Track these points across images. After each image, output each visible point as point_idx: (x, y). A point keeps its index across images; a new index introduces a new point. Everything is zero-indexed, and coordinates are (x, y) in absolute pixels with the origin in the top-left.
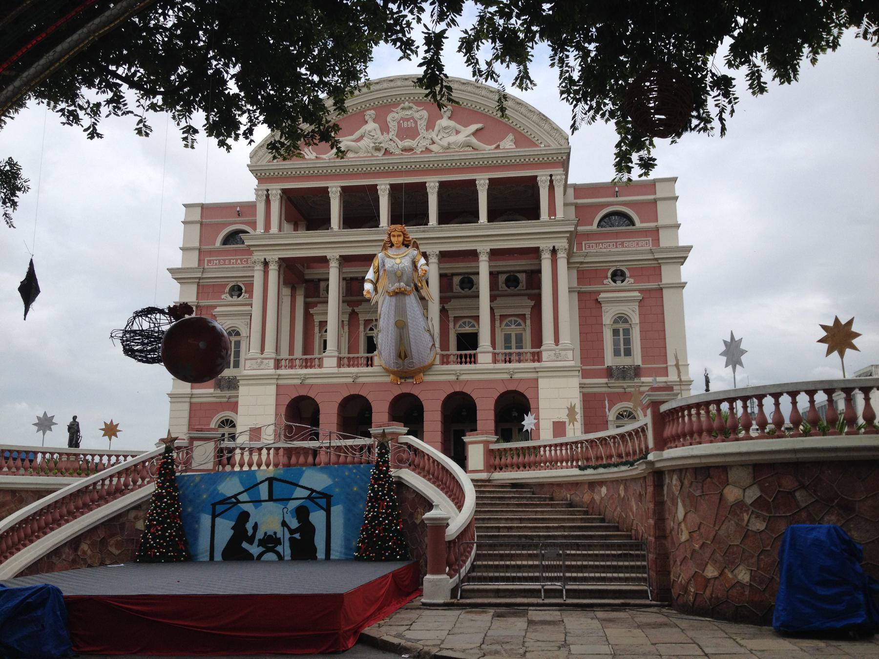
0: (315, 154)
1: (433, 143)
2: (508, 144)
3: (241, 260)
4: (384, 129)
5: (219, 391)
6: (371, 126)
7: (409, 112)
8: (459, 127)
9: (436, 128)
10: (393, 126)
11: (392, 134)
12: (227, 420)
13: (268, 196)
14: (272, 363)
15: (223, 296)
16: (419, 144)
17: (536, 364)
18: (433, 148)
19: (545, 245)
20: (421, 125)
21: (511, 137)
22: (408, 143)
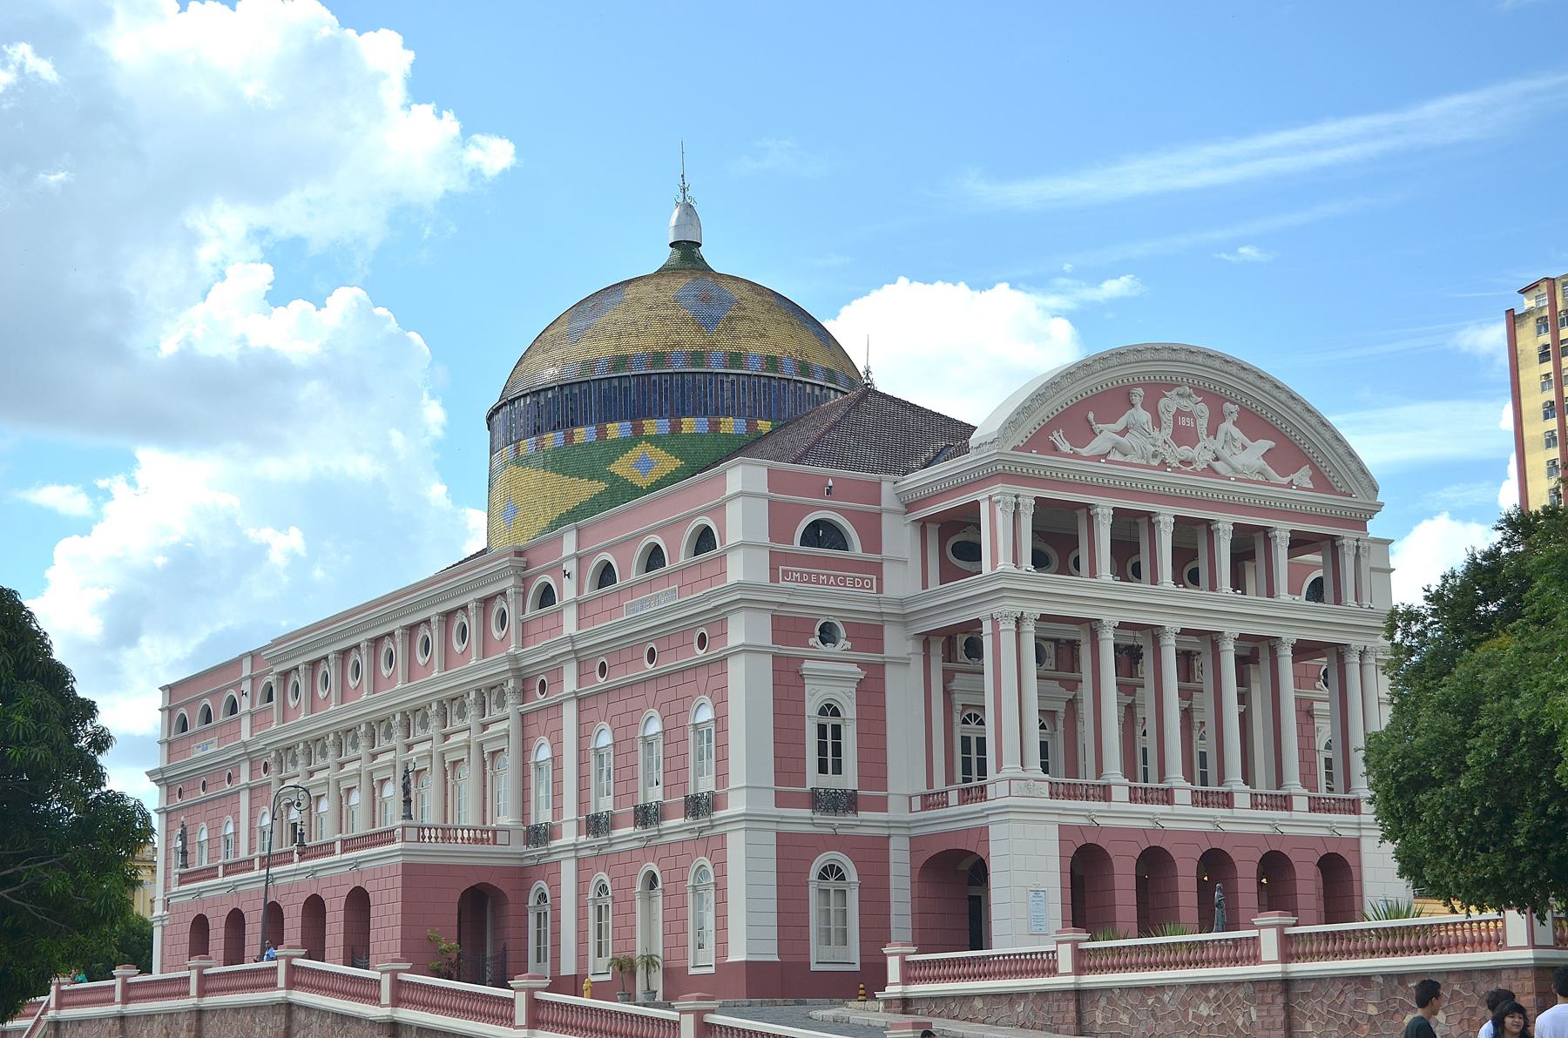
0: (1065, 447)
1: (1217, 459)
2: (1303, 476)
3: (836, 577)
4: (1157, 422)
5: (818, 815)
6: (1142, 416)
7: (1184, 402)
8: (1247, 441)
9: (1221, 435)
10: (1167, 419)
11: (1167, 432)
12: (832, 866)
13: (1017, 505)
14: (1045, 787)
15: (812, 641)
16: (1201, 454)
17: (1353, 818)
18: (1218, 466)
19: (1356, 642)
20: (1203, 424)
21: (1306, 471)
22: (1185, 451)
